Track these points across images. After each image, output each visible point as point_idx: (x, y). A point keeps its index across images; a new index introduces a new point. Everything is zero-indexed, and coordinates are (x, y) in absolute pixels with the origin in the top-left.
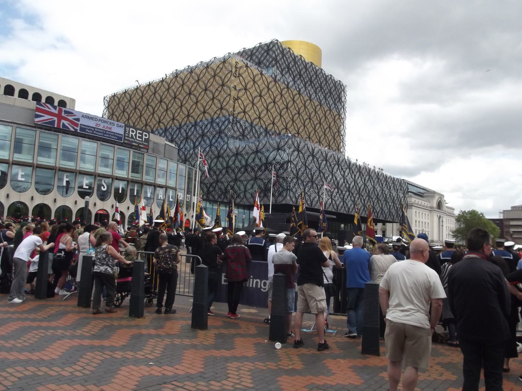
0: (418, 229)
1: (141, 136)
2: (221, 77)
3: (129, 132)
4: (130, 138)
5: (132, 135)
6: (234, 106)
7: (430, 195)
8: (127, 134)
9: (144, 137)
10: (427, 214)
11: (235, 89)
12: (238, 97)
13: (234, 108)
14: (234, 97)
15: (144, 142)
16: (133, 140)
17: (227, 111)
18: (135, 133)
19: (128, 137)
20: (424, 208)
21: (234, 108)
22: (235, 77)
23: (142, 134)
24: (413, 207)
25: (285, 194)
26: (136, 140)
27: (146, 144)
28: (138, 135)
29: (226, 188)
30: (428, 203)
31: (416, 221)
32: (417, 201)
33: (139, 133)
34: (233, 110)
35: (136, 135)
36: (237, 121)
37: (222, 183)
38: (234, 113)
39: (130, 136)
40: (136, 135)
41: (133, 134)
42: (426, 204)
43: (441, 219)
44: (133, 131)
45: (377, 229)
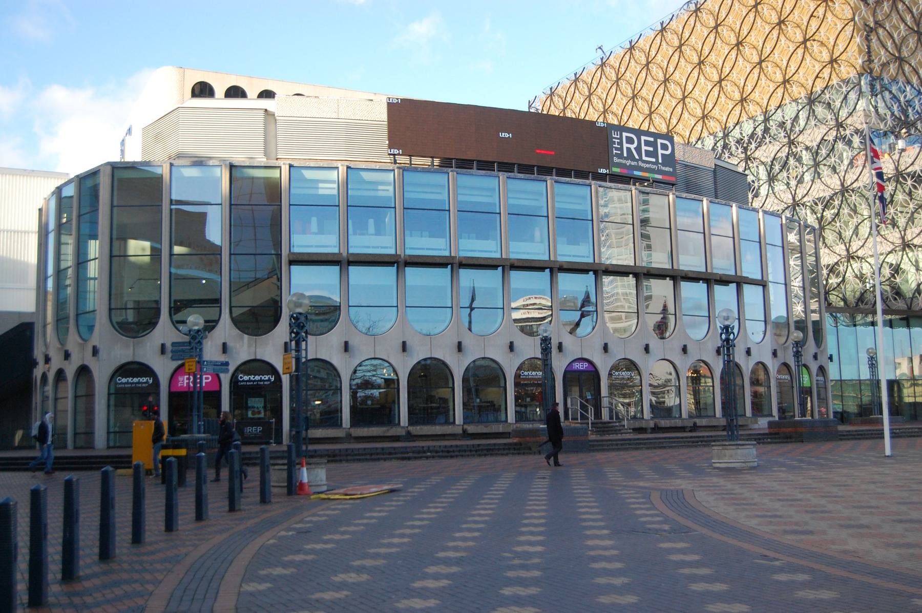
1: (651, 149)
3: (621, 143)
4: (626, 159)
8: (617, 149)
9: (660, 152)
15: (663, 164)
16: (633, 163)
18: (635, 145)
19: (620, 156)
23: (654, 144)
26: (640, 163)
27: (667, 169)
28: (644, 148)
33: (647, 143)
35: (638, 149)
39: (625, 155)
40: (638, 149)
44: (629, 140)
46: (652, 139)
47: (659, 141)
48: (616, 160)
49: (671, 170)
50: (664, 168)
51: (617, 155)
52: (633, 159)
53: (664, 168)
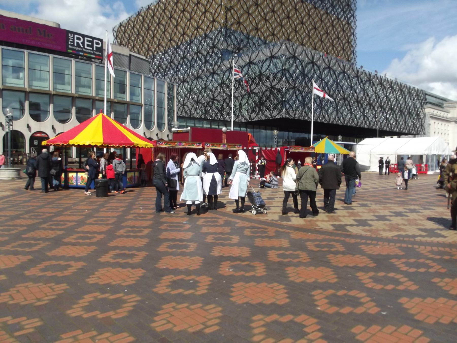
1: (90, 44)
3: (73, 40)
5: (78, 43)
6: (226, 16)
8: (71, 42)
9: (95, 45)
15: (96, 51)
16: (80, 49)
17: (219, 23)
19: (73, 45)
21: (226, 19)
23: (92, 42)
27: (98, 53)
28: (86, 43)
29: (222, 106)
33: (88, 41)
34: (225, 21)
35: (83, 43)
37: (218, 101)
39: (76, 45)
41: (80, 42)
44: (78, 39)
46: (91, 40)
47: (95, 41)
48: (70, 47)
49: (100, 54)
50: (96, 53)
51: (71, 45)
52: (79, 47)
53: (96, 53)
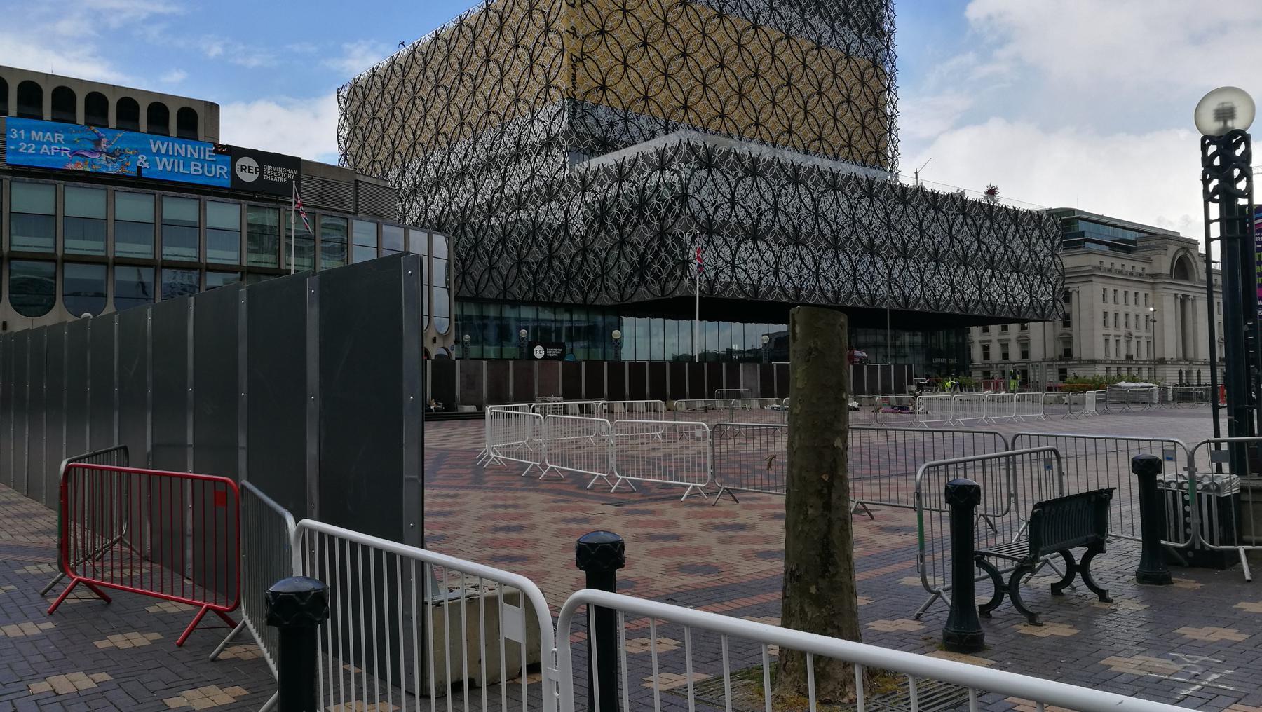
0: (1112, 331)
2: (543, 12)
6: (574, 75)
7: (1152, 243)
10: (1141, 294)
11: (575, 35)
12: (582, 53)
13: (574, 80)
14: (572, 55)
20: (1131, 278)
21: (574, 80)
22: (572, 6)
24: (1094, 279)
25: (678, 273)
30: (1146, 266)
31: (1105, 314)
32: (1107, 262)
34: (571, 86)
36: (583, 110)
38: (575, 93)
42: (1139, 267)
43: (1189, 304)
45: (1009, 340)
